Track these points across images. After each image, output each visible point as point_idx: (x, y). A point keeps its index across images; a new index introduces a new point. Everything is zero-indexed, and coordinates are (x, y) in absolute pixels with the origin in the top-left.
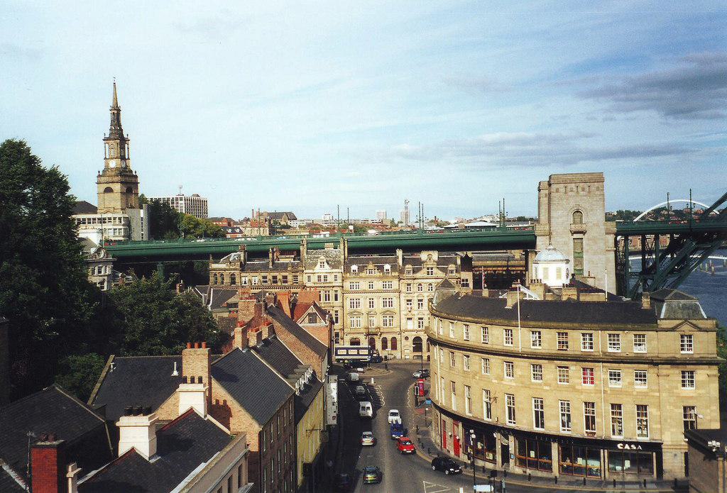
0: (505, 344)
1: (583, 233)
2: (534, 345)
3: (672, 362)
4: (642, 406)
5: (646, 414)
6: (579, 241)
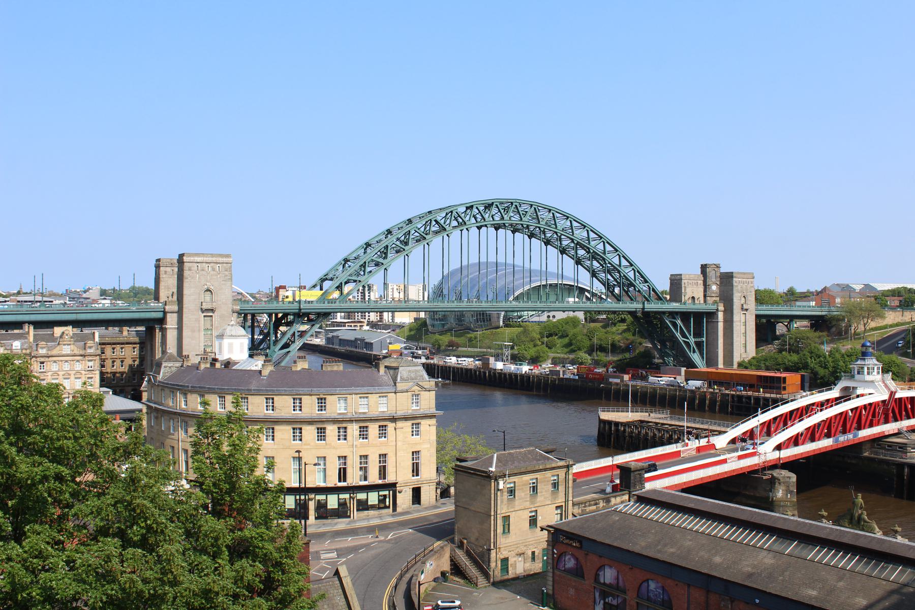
0: (266, 412)
1: (212, 310)
2: (294, 410)
3: (406, 418)
4: (364, 456)
5: (367, 462)
6: (209, 318)
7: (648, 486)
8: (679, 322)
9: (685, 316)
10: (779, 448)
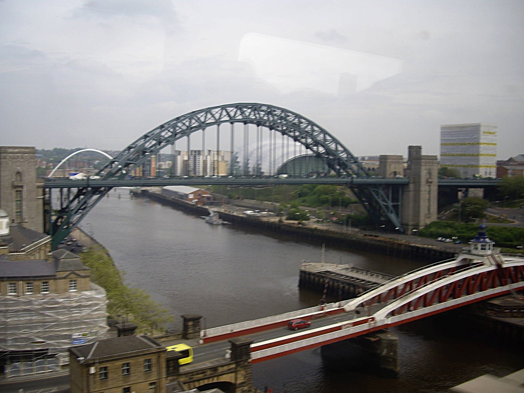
1: (22, 187)
7: (255, 355)
8: (381, 192)
9: (387, 186)
10: (393, 313)
